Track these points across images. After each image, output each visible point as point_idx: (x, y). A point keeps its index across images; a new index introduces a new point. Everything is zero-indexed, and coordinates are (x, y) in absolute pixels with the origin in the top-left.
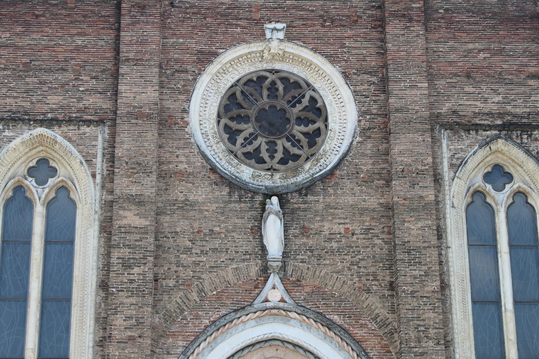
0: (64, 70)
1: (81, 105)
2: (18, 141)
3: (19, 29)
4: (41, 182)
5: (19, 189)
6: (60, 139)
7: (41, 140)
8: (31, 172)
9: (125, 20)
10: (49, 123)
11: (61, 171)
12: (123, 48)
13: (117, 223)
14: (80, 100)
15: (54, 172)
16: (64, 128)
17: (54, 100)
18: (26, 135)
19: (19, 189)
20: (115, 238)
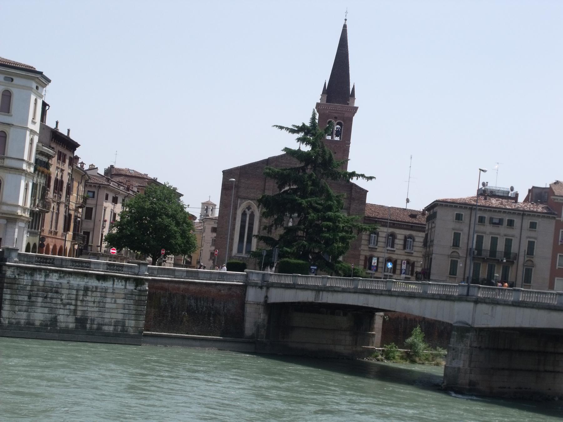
0: (254, 189)
1: (257, 196)
2: (245, 203)
3: (246, 180)
4: (249, 210)
5: (244, 211)
6: (253, 203)
7: (249, 202)
8: (247, 208)
9: (267, 181)
10: (252, 200)
11: (252, 208)
12: (266, 187)
13: (262, 221)
14: (257, 195)
15: (251, 208)
16: (254, 201)
17: (252, 195)
18: (247, 202)
19: (244, 211)
20: (261, 224)
